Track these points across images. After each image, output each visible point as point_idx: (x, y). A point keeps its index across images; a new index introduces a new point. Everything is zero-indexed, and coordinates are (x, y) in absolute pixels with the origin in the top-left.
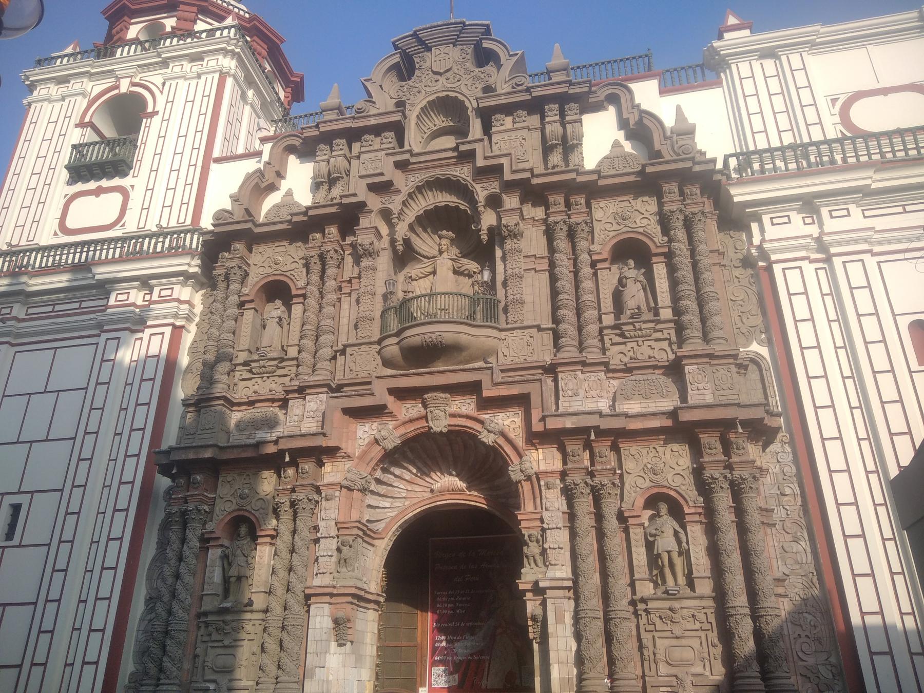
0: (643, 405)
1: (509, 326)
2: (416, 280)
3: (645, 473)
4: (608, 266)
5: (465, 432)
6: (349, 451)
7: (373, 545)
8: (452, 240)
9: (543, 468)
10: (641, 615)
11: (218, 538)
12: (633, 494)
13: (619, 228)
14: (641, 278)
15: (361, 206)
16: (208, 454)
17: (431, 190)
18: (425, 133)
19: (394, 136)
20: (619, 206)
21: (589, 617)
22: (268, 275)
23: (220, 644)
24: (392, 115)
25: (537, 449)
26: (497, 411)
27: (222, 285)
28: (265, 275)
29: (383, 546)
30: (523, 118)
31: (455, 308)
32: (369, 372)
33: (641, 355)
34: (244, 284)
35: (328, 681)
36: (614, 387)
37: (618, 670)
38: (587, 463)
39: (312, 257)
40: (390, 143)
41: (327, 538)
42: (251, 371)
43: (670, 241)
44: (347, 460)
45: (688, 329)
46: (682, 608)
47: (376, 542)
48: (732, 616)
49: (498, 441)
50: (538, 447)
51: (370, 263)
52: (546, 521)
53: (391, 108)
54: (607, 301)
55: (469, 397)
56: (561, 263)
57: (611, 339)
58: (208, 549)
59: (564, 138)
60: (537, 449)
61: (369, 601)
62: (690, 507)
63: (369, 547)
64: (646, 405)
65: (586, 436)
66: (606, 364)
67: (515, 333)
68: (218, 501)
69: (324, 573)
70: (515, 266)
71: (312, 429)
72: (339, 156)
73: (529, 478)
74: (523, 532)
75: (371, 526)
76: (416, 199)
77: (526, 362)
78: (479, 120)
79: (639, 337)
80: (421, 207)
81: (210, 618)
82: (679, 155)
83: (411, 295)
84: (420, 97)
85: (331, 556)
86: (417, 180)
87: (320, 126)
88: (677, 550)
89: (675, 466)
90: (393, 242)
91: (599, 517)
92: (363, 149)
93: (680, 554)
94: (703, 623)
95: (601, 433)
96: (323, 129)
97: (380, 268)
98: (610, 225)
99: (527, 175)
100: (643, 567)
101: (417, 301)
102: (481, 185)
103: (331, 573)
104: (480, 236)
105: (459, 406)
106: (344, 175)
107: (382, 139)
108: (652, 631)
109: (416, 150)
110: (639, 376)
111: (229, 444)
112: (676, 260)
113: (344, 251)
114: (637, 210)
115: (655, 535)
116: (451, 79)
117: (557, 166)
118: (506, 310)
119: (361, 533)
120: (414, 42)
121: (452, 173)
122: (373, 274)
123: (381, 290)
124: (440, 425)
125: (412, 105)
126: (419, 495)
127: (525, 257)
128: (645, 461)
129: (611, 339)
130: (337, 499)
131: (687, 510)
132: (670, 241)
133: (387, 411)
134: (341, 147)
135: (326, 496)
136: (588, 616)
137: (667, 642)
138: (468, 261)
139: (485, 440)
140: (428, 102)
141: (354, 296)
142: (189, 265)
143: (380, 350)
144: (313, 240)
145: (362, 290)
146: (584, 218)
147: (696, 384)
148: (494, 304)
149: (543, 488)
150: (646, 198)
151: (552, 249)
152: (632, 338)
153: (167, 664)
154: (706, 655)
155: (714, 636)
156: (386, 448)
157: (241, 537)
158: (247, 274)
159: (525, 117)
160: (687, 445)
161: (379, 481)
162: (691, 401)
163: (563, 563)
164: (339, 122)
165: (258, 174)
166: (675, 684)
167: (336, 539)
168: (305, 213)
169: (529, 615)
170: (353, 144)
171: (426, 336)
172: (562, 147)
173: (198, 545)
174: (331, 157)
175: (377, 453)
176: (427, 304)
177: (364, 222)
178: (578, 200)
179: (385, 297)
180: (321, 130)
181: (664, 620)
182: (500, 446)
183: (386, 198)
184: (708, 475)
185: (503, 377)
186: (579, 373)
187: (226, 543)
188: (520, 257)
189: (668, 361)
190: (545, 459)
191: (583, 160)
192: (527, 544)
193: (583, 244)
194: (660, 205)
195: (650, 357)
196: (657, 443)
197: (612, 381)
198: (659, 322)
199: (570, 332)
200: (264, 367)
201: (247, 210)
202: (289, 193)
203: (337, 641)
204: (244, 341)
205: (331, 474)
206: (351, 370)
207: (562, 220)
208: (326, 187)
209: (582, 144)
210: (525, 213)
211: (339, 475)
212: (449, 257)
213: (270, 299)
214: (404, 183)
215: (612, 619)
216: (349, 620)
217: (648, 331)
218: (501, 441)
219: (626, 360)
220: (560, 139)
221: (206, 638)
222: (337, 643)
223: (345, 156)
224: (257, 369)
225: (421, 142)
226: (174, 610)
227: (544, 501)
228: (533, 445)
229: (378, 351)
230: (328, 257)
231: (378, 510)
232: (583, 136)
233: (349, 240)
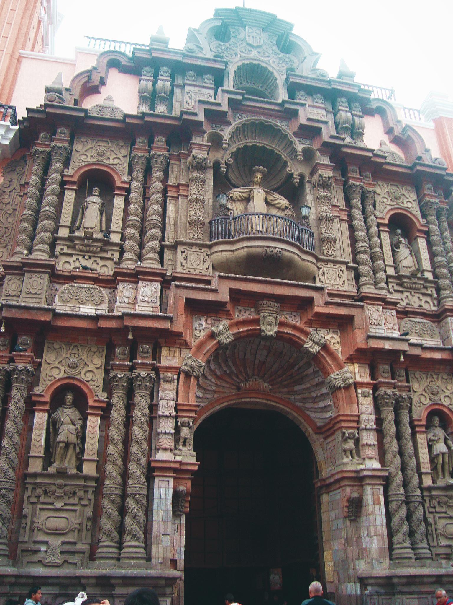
5: (291, 339)
6: (188, 339)
9: (359, 379)
25: (353, 363)
32: (201, 271)
37: (418, 541)
42: (73, 247)
51: (202, 176)
52: (363, 423)
56: (360, 218)
58: (33, 412)
68: (44, 366)
79: (413, 288)
81: (39, 480)
84: (237, 58)
86: (244, 119)
89: (445, 390)
91: (398, 422)
97: (206, 183)
98: (385, 200)
102: (298, 139)
115: (433, 440)
124: (271, 330)
127: (332, 206)
128: (426, 384)
130: (176, 382)
132: (427, 223)
138: (280, 196)
139: (311, 350)
149: (360, 396)
150: (409, 188)
152: (407, 288)
157: (69, 405)
177: (196, 140)
180: (153, 55)
182: (322, 355)
186: (381, 308)
195: (420, 306)
200: (88, 246)
204: (66, 218)
205: (169, 358)
211: (176, 359)
217: (419, 286)
219: (403, 304)
221: (35, 500)
224: (81, 247)
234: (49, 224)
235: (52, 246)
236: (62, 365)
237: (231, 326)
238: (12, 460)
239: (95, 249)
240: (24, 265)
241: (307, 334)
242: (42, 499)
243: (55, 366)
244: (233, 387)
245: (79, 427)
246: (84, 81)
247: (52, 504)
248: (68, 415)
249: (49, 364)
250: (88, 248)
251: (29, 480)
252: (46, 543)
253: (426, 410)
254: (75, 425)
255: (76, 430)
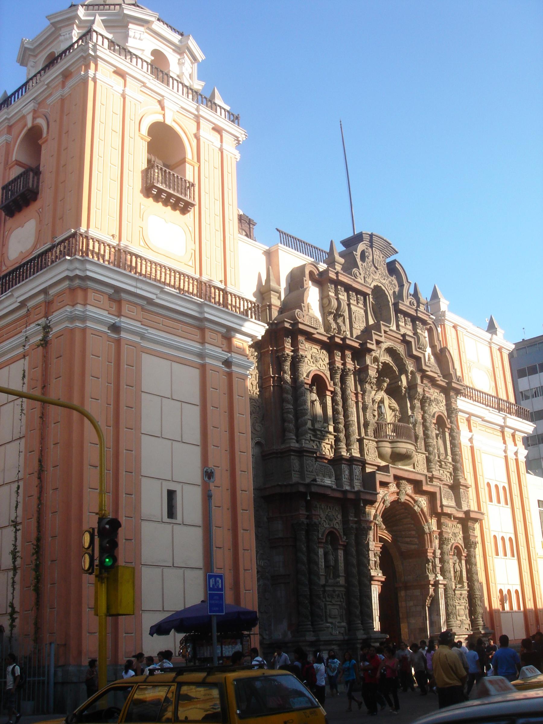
5: (408, 504)
116: (381, 276)
120: (367, 239)
164: (347, 278)
214: (384, 346)
252: (331, 623)
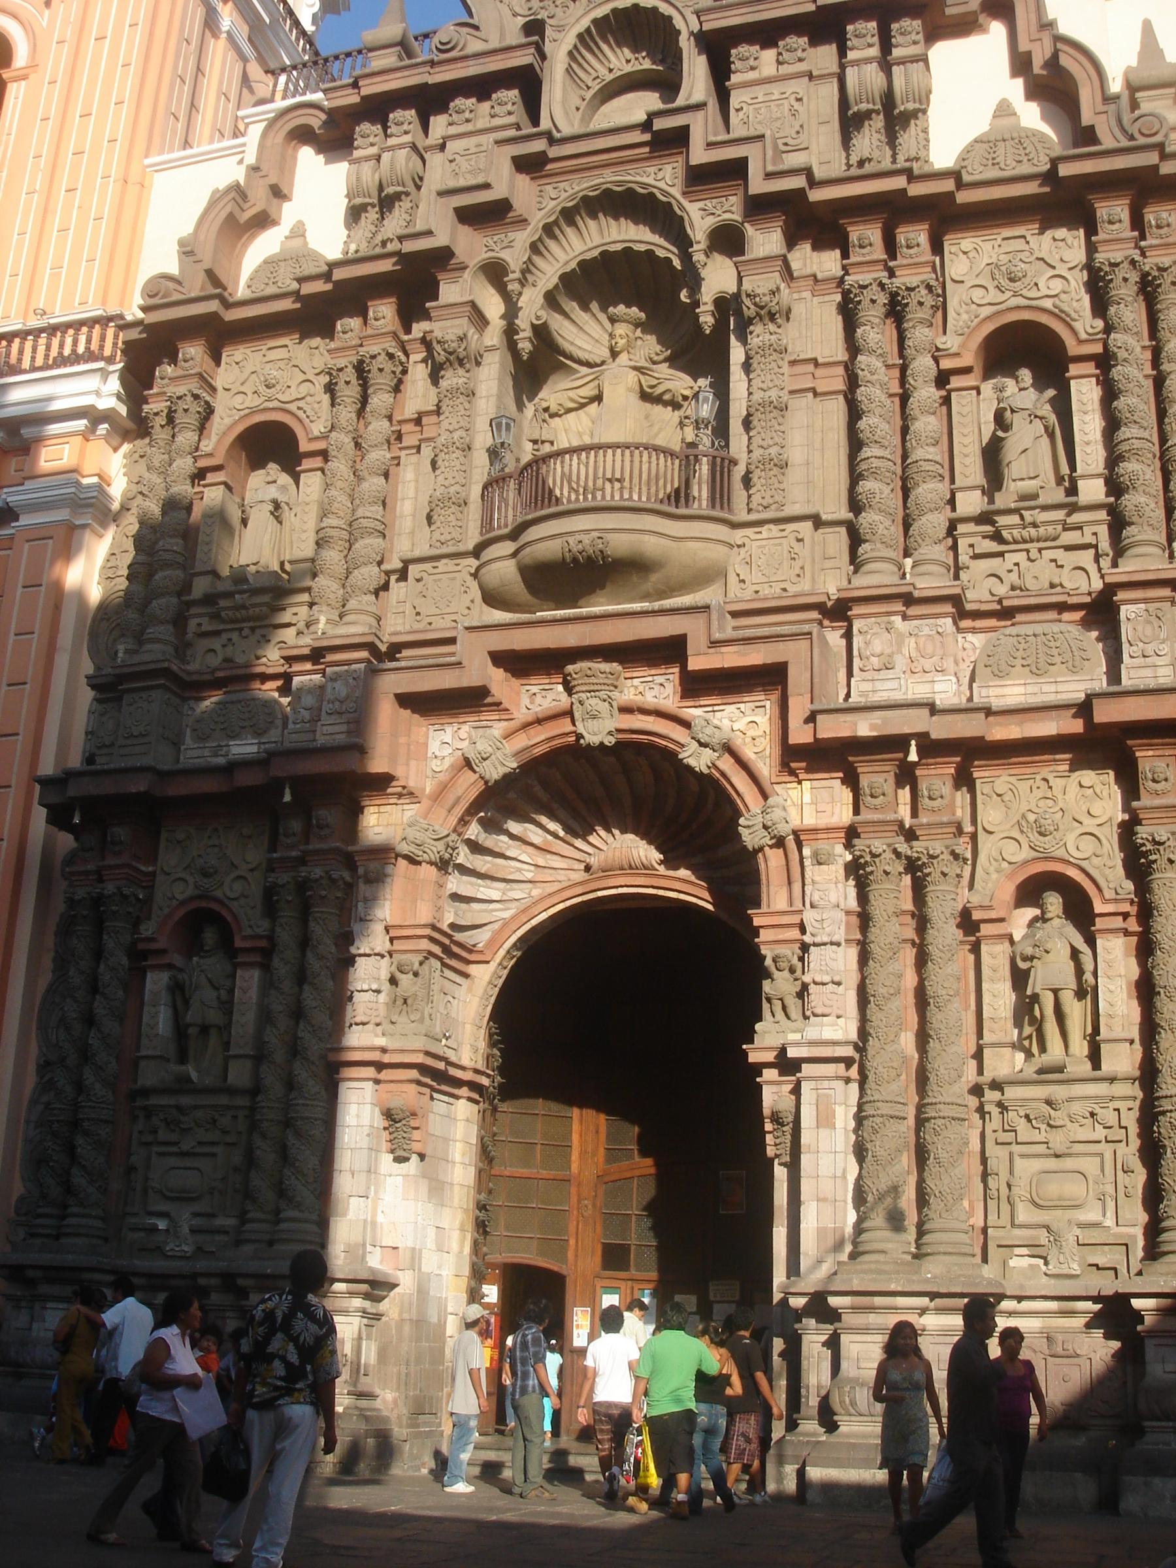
0: (1030, 689)
1: (754, 517)
2: (560, 416)
3: (1022, 832)
4: (973, 383)
6: (412, 784)
7: (466, 976)
8: (637, 325)
9: (810, 820)
10: (989, 1113)
11: (163, 952)
12: (994, 876)
13: (1002, 297)
14: (1047, 410)
15: (442, 258)
16: (139, 785)
17: (594, 217)
18: (589, 88)
19: (518, 100)
20: (1002, 250)
21: (882, 1116)
22: (254, 411)
23: (174, 1149)
24: (514, 54)
25: (800, 782)
26: (719, 702)
27: (160, 434)
28: (247, 411)
29: (487, 978)
30: (799, 54)
31: (645, 476)
32: (454, 617)
33: (1034, 581)
34: (205, 432)
35: (374, 1224)
36: (975, 648)
37: (931, 1215)
38: (904, 812)
39: (340, 370)
40: (510, 113)
41: (369, 955)
43: (1108, 329)
44: (407, 801)
45: (1133, 524)
46: (1070, 1100)
47: (473, 969)
48: (1163, 1113)
49: (720, 764)
50: (801, 776)
51: (461, 381)
52: (809, 929)
53: (514, 36)
54: (967, 461)
55: (663, 671)
57: (972, 546)
58: (143, 973)
59: (888, 99)
60: (800, 782)
61: (458, 1083)
62: (1107, 901)
63: (458, 979)
64: (1036, 689)
65: (901, 755)
66: (956, 600)
67: (766, 531)
68: (160, 878)
69: (364, 1024)
70: (771, 385)
71: (337, 736)
72: (401, 146)
73: (780, 843)
74: (763, 952)
75: (458, 937)
76: (561, 237)
77: (785, 594)
78: (703, 59)
79: (1032, 541)
80: (572, 255)
81: (154, 1101)
82: (1132, 138)
83: (547, 449)
85: (378, 991)
86: (564, 195)
87: (360, 84)
88: (1075, 988)
90: (510, 332)
92: (453, 130)
93: (1080, 994)
94: (1110, 1127)
95: (932, 748)
96: (370, 88)
98: (977, 294)
99: (798, 182)
100: (1003, 1022)
101: (562, 462)
102: (701, 204)
103: (378, 1025)
104: (697, 317)
105: (641, 689)
106: (411, 188)
107: (493, 107)
108: (1010, 1144)
109: (566, 129)
110: (1026, 626)
111: (180, 766)
112: (1115, 373)
113: (407, 356)
114: (1042, 259)
115: (1032, 958)
117: (870, 160)
118: (747, 481)
119: (437, 950)
121: (638, 179)
122: (467, 405)
123: (483, 439)
125: (560, 29)
126: (561, 875)
127: (793, 363)
128: (1024, 807)
129: (972, 546)
131: (1099, 907)
132: (1108, 329)
133: (489, 700)
134: (405, 127)
135: (366, 872)
136: (879, 1112)
137: (1037, 1165)
139: (692, 762)
140: (595, 22)
141: (427, 452)
142: (97, 393)
143: (478, 569)
144: (344, 333)
145: (442, 440)
146: (924, 277)
147: (1141, 645)
148: (722, 468)
149: (807, 862)
150: (1062, 233)
151: (853, 347)
152: (1016, 542)
153: (79, 1179)
154: (1110, 1189)
155: (1130, 1151)
156: (487, 777)
157: (207, 951)
158: (209, 411)
159: (804, 50)
160: (1112, 773)
161: (475, 847)
162: (1127, 682)
163: (840, 1012)
165: (233, 194)
166: (1043, 1241)
167: (387, 958)
168: (327, 276)
169: (766, 1111)
170: (432, 118)
171: (571, 540)
172: (881, 116)
173: (125, 961)
174: (383, 150)
175: (468, 788)
176: (582, 467)
177: (450, 291)
178: (911, 235)
179: (494, 454)
180: (365, 91)
181: (1034, 1122)
183: (496, 238)
184: (1144, 836)
185: (735, 628)
186: (897, 620)
187: (177, 960)
188: (780, 363)
189: (1090, 594)
190: (814, 802)
191: (926, 148)
192: (768, 975)
193: (919, 335)
194: (1091, 249)
195: (1052, 586)
196: (1051, 768)
197: (970, 637)
198: (1073, 508)
199: (881, 530)
200: (244, 607)
201: (210, 274)
202: (299, 232)
203: (392, 1151)
206: (418, 614)
207: (875, 280)
208: (373, 214)
209: (924, 112)
210: (795, 265)
212: (632, 364)
213: (257, 463)
215: (928, 1120)
216: (414, 1114)
217: (1050, 529)
218: (726, 764)
219: (1002, 590)
220: (878, 100)
221: (150, 1138)
222: (391, 1156)
223: (414, 147)
224: (230, 613)
225: (578, 109)
226: (87, 1082)
227: (808, 889)
228: (793, 773)
229: (473, 571)
230: (374, 370)
231: (475, 906)
232: (930, 92)
233: (418, 329)
234: (165, 578)
235: (179, 621)
236: (191, 874)
237: (507, 736)
238: (101, 1068)
239: (257, 610)
240: (121, 678)
241: (686, 724)
242: (162, 1135)
243: (178, 876)
244: (577, 866)
245: (223, 993)
246: (224, 214)
247: (176, 1144)
248: (202, 971)
249: (169, 874)
250: (244, 612)
251: (140, 1102)
253: (1010, 877)
254: (217, 989)
255: (218, 998)
